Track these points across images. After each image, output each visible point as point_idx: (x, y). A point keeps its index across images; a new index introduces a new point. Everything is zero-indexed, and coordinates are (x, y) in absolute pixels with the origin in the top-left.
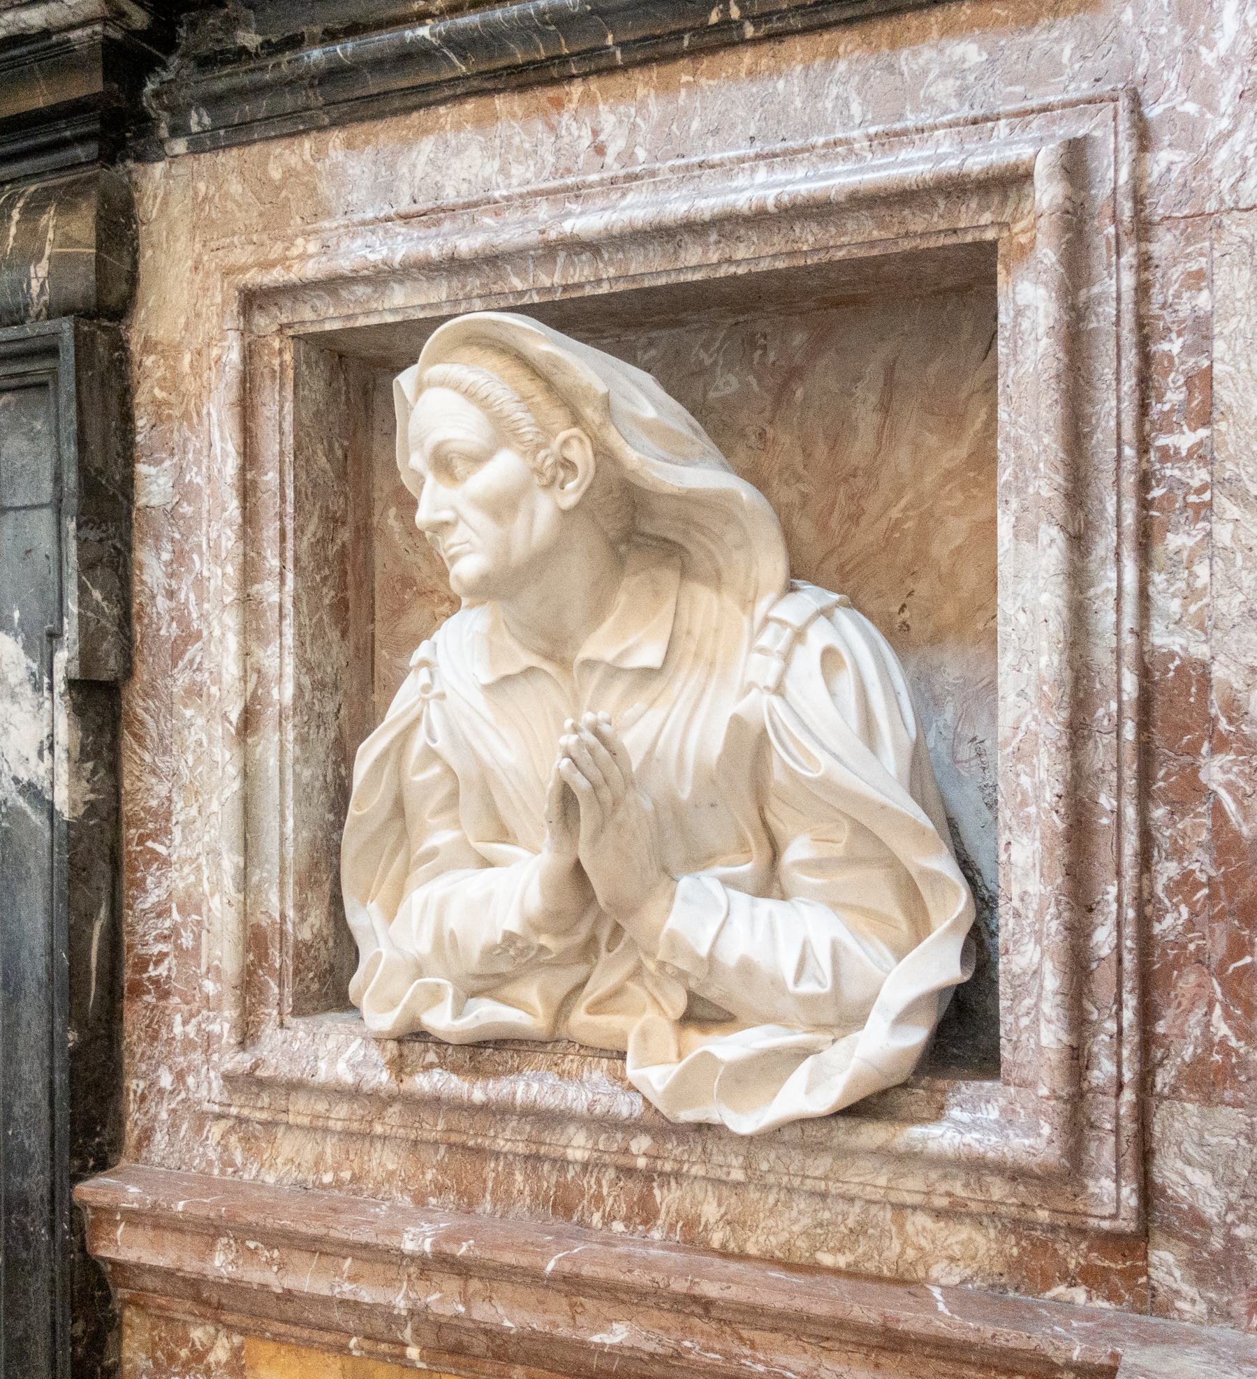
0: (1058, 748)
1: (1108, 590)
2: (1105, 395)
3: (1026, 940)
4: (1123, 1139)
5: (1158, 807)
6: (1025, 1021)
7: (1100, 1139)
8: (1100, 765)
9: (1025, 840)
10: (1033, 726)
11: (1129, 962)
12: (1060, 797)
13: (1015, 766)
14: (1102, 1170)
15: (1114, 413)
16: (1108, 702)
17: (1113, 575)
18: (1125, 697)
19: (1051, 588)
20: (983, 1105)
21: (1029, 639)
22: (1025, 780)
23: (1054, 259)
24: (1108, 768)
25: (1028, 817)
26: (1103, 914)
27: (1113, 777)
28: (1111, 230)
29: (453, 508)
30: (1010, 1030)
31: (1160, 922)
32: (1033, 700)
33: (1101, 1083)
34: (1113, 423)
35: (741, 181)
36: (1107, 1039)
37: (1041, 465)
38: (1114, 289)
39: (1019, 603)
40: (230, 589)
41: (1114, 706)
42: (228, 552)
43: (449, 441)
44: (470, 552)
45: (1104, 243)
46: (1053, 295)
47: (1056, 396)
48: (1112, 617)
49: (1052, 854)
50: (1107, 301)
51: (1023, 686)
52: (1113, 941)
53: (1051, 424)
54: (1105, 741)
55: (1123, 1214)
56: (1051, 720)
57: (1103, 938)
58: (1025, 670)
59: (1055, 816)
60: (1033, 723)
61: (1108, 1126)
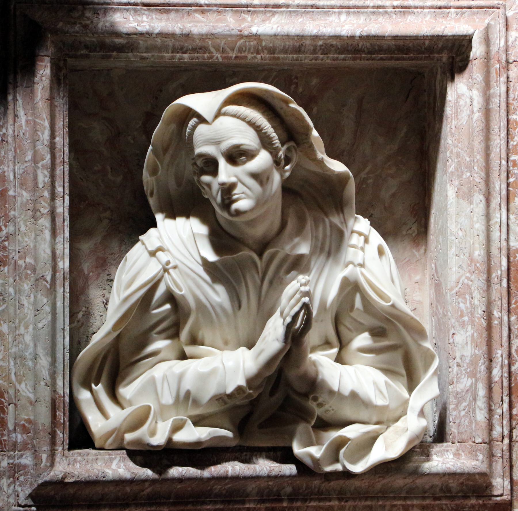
0: (483, 291)
1: (496, 222)
2: (495, 138)
3: (463, 377)
4: (505, 460)
5: (513, 316)
6: (463, 413)
7: (496, 461)
8: (494, 298)
9: (462, 332)
10: (466, 281)
11: (506, 383)
12: (484, 312)
13: (457, 299)
14: (497, 474)
15: (499, 146)
16: (497, 271)
17: (498, 216)
18: (503, 269)
19: (480, 221)
20: (446, 453)
21: (464, 243)
22: (462, 305)
23: (481, 79)
24: (497, 299)
25: (464, 322)
26: (496, 363)
27: (499, 303)
28: (497, 66)
29: (236, 176)
30: (455, 418)
31: (514, 366)
32: (465, 269)
33: (496, 436)
34: (498, 150)
35: (333, 18)
36: (498, 417)
37: (476, 168)
38: (499, 91)
39: (459, 226)
40: (46, 205)
41: (499, 272)
42: (45, 183)
43: (242, 145)
44: (244, 198)
45: (495, 71)
46: (481, 94)
47: (482, 138)
48: (498, 234)
49: (481, 337)
50: (496, 97)
51: (461, 263)
52: (500, 374)
53: (480, 150)
54: (496, 288)
55: (505, 493)
56: (481, 279)
57: (496, 372)
58: (462, 256)
59: (482, 320)
60: (466, 280)
61: (499, 455)
